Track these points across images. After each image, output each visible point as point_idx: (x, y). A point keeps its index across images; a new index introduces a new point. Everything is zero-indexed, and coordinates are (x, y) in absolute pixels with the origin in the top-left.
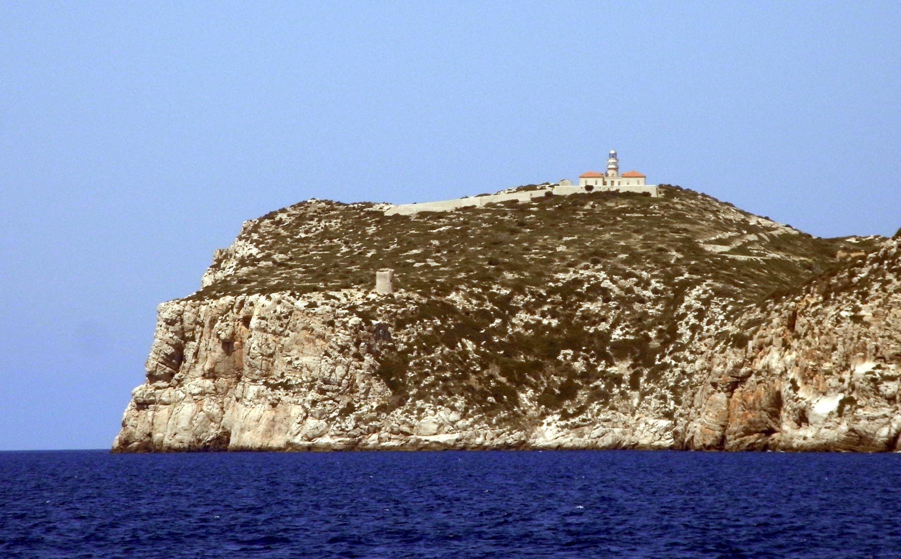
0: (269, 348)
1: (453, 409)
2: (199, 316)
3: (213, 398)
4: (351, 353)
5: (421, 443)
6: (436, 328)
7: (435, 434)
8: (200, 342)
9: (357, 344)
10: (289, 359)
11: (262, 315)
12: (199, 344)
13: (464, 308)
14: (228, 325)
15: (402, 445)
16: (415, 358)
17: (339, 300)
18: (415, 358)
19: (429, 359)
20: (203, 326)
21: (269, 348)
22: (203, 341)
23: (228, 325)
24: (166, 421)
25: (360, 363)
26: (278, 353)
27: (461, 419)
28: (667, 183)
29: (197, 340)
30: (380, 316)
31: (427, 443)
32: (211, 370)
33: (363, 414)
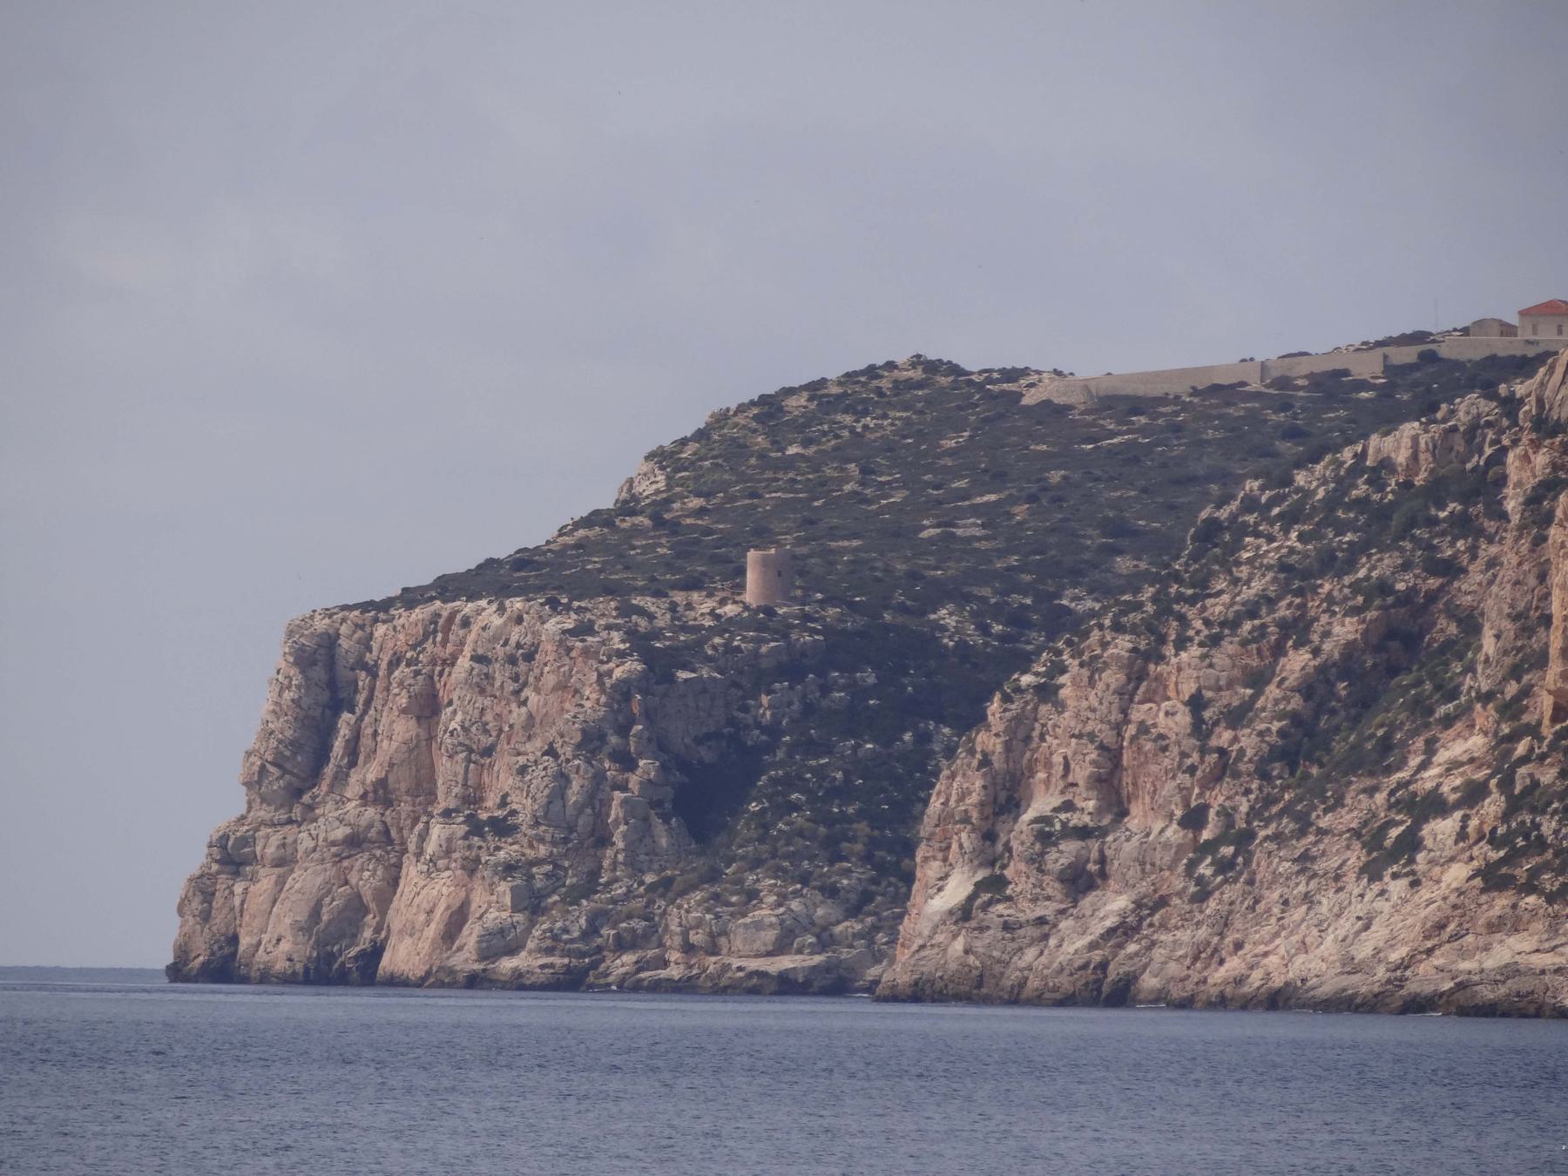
0: (486, 732)
1: (831, 892)
2: (370, 649)
3: (378, 853)
4: (607, 749)
5: (729, 974)
6: (858, 692)
7: (769, 954)
8: (365, 712)
9: (623, 731)
10: (522, 760)
11: (480, 651)
12: (360, 719)
13: (962, 645)
14: (417, 673)
15: (690, 978)
16: (781, 764)
17: (651, 617)
18: (781, 764)
19: (811, 770)
20: (375, 676)
21: (486, 732)
22: (372, 712)
23: (417, 673)
24: (266, 906)
25: (1097, 744)
26: (503, 745)
27: (846, 919)
28: (1001, 367)
29: (358, 711)
30: (709, 659)
31: (741, 974)
32: (382, 783)
33: (614, 901)
